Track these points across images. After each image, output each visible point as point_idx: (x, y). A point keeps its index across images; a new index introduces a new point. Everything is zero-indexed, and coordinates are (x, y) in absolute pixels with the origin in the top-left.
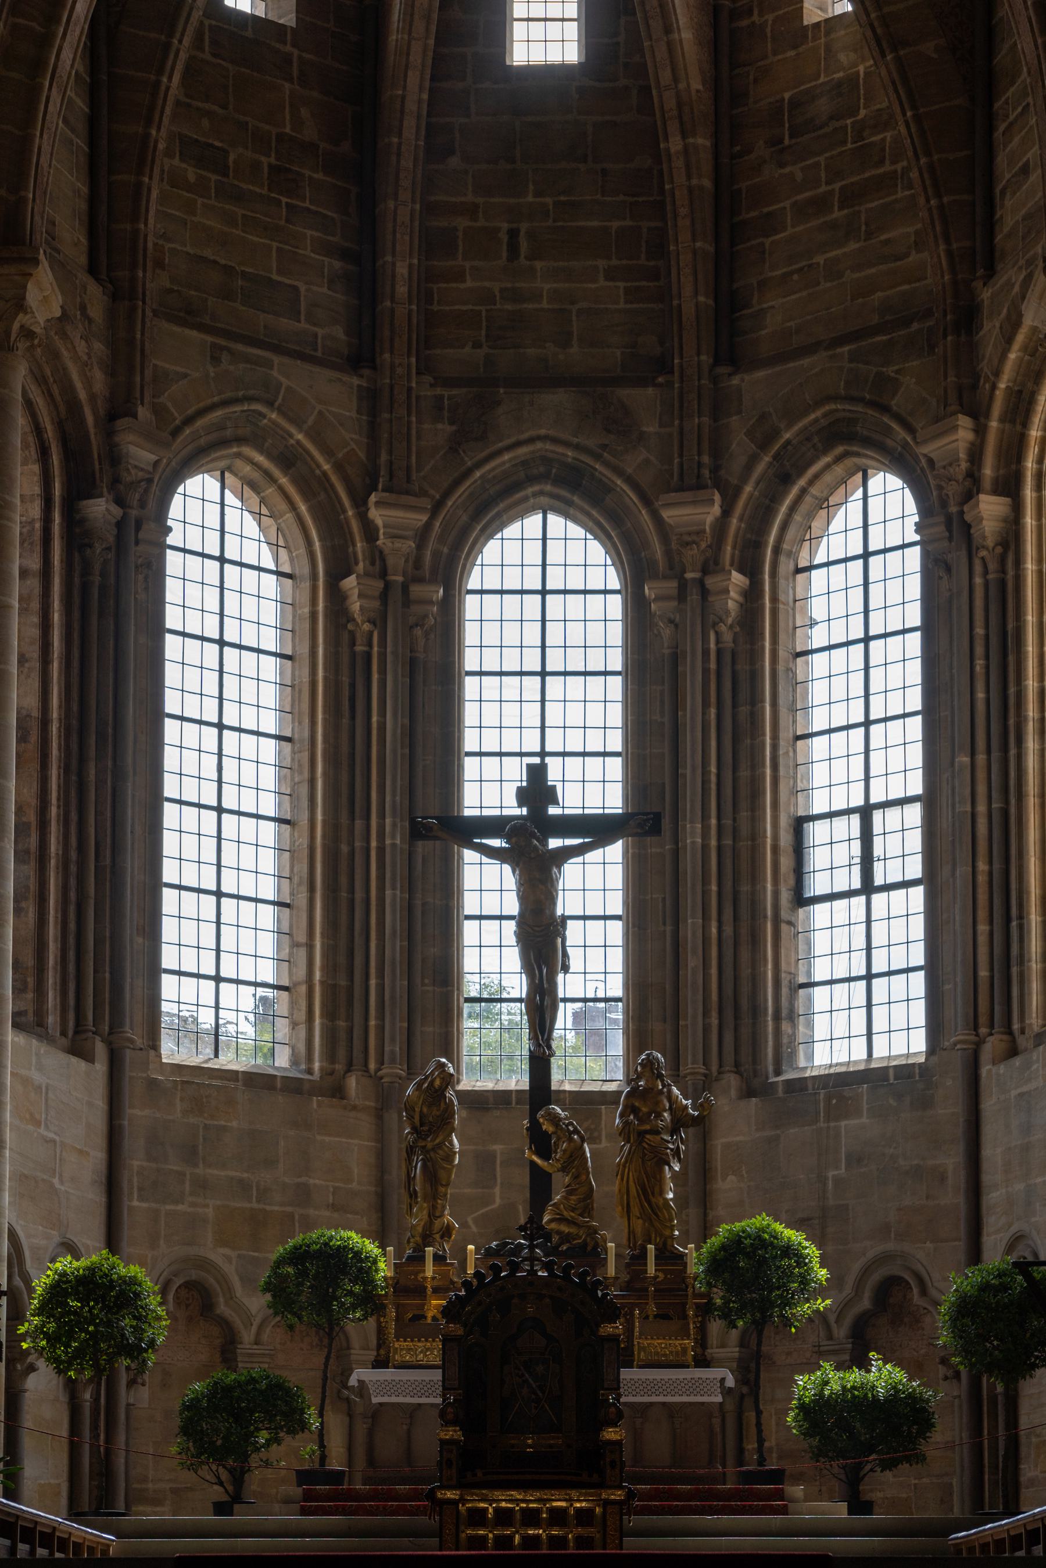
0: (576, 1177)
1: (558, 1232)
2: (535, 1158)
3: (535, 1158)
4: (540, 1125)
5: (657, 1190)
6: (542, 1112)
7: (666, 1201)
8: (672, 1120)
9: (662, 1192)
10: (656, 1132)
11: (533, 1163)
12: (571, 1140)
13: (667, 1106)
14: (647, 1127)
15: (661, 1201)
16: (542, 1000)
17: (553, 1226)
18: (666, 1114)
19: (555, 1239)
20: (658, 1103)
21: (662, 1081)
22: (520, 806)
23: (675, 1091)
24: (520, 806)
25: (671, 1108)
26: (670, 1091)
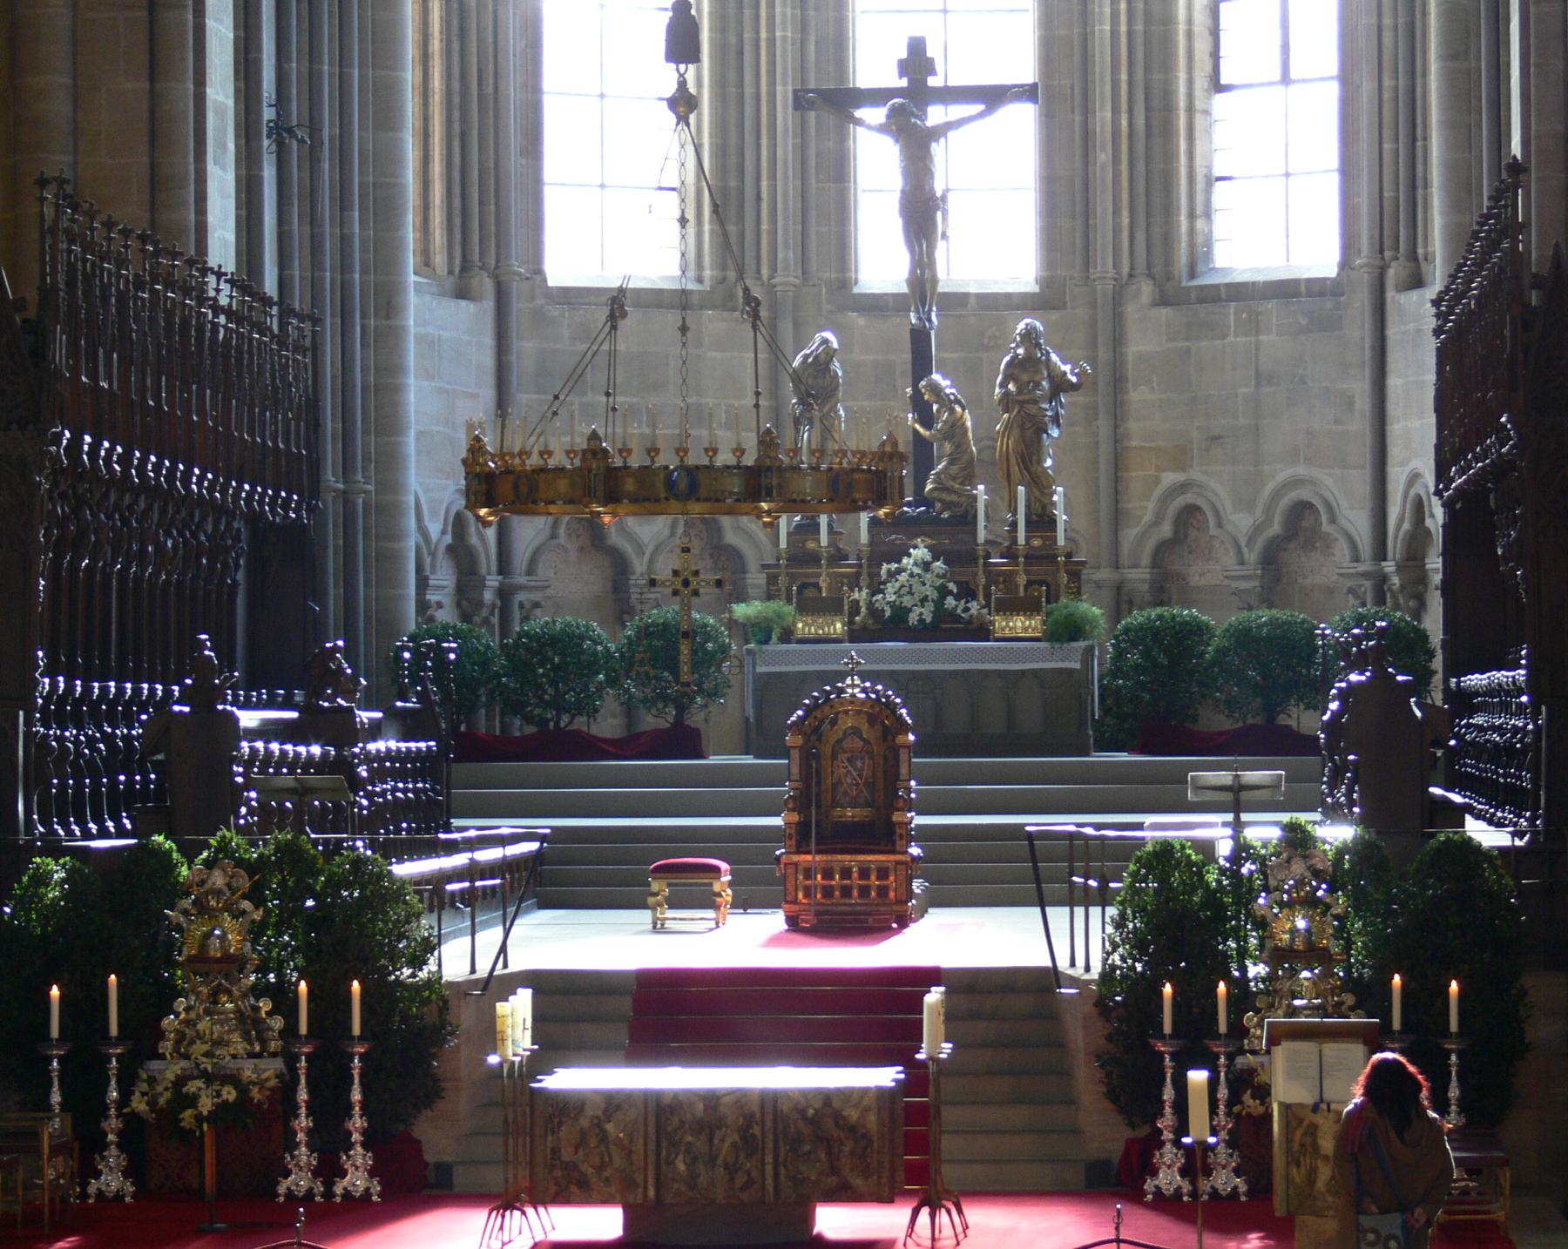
0: (958, 446)
1: (941, 501)
2: (917, 426)
3: (917, 426)
4: (922, 395)
5: (1034, 458)
6: (923, 383)
7: (1045, 469)
8: (1051, 387)
9: (1040, 462)
10: (1035, 402)
11: (916, 432)
12: (952, 411)
13: (1046, 373)
14: (1026, 397)
15: (1039, 468)
16: (923, 273)
17: (936, 494)
18: (1044, 383)
19: (938, 505)
20: (1038, 372)
21: (1041, 349)
22: (901, 76)
23: (1054, 357)
24: (901, 76)
25: (1049, 375)
26: (1048, 359)
